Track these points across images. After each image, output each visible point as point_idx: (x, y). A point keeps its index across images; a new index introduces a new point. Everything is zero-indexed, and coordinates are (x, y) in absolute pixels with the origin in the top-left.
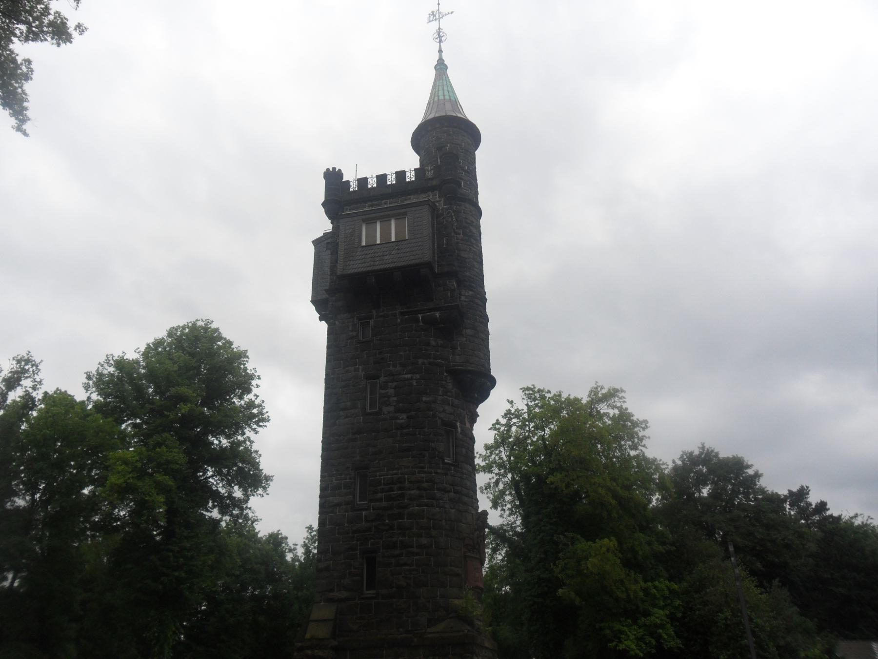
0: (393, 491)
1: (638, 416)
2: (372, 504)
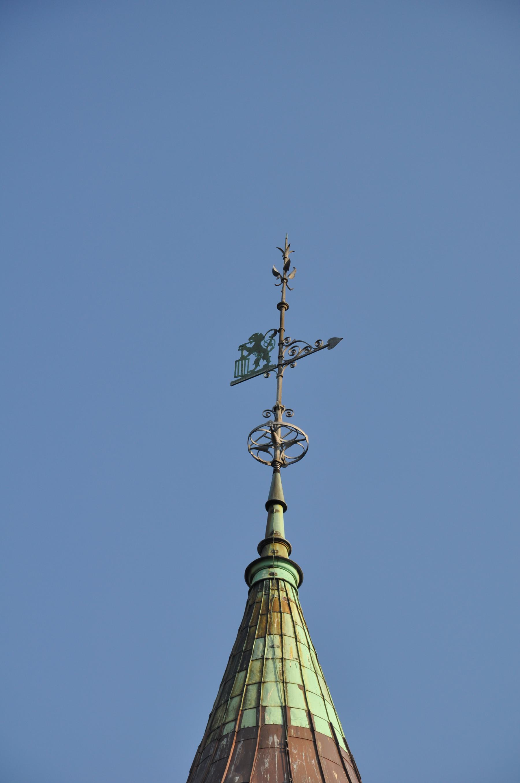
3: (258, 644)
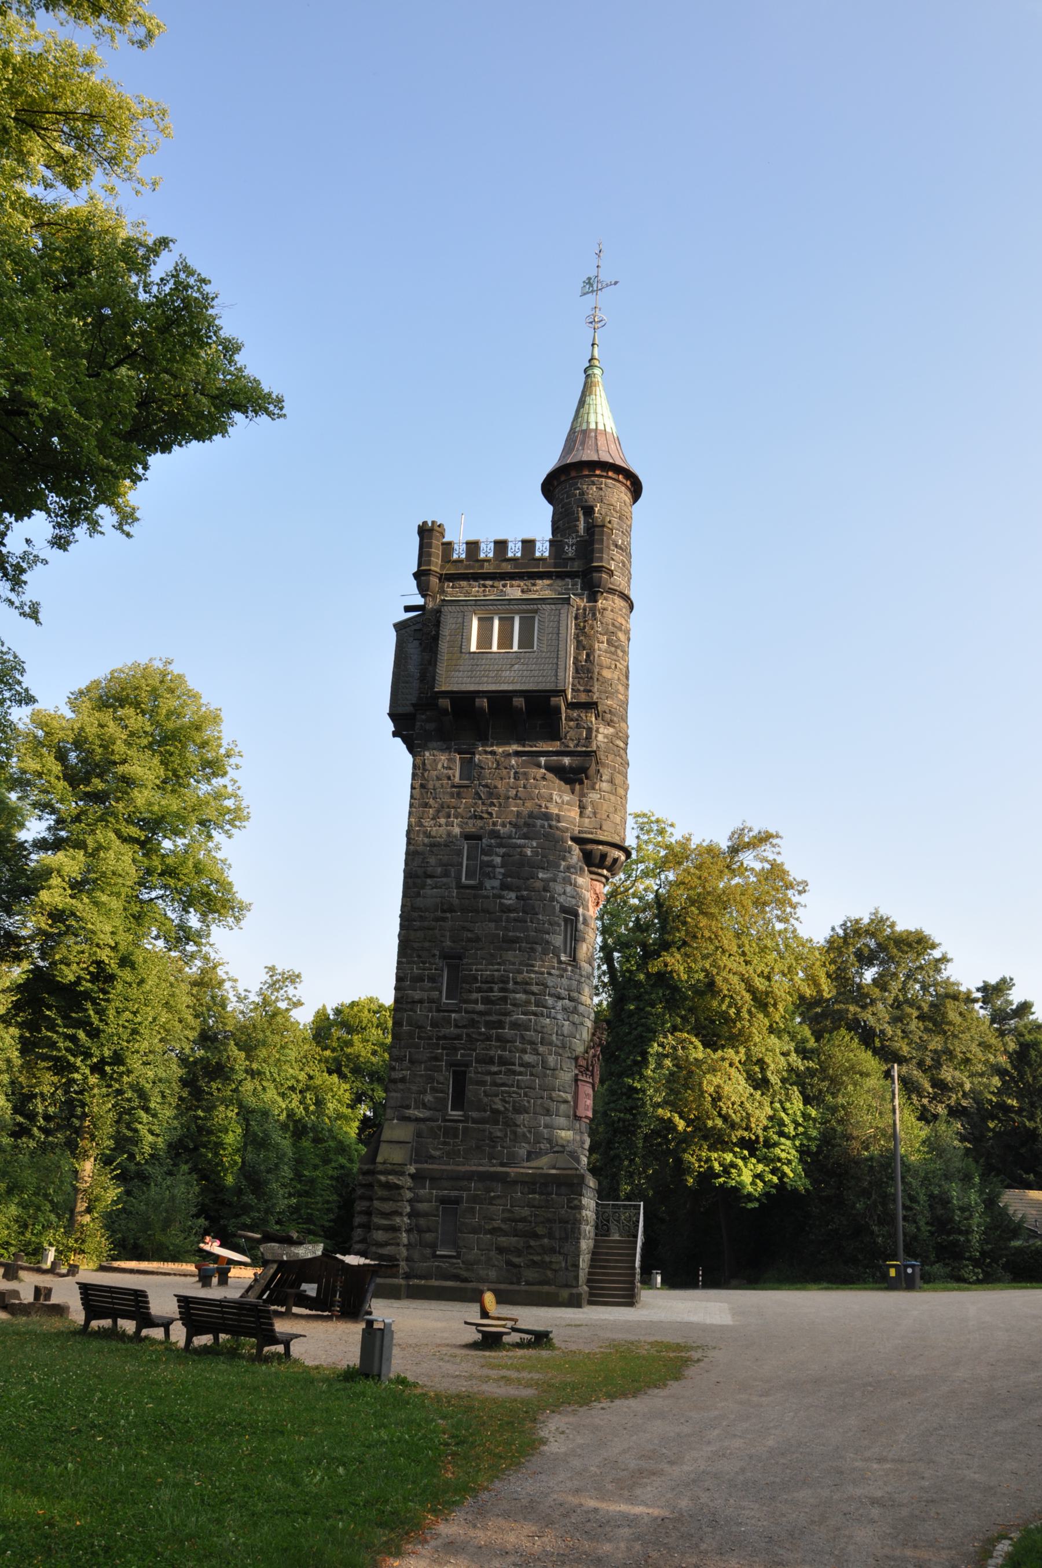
0: (492, 991)
1: (795, 872)
2: (464, 1006)
3: (587, 398)
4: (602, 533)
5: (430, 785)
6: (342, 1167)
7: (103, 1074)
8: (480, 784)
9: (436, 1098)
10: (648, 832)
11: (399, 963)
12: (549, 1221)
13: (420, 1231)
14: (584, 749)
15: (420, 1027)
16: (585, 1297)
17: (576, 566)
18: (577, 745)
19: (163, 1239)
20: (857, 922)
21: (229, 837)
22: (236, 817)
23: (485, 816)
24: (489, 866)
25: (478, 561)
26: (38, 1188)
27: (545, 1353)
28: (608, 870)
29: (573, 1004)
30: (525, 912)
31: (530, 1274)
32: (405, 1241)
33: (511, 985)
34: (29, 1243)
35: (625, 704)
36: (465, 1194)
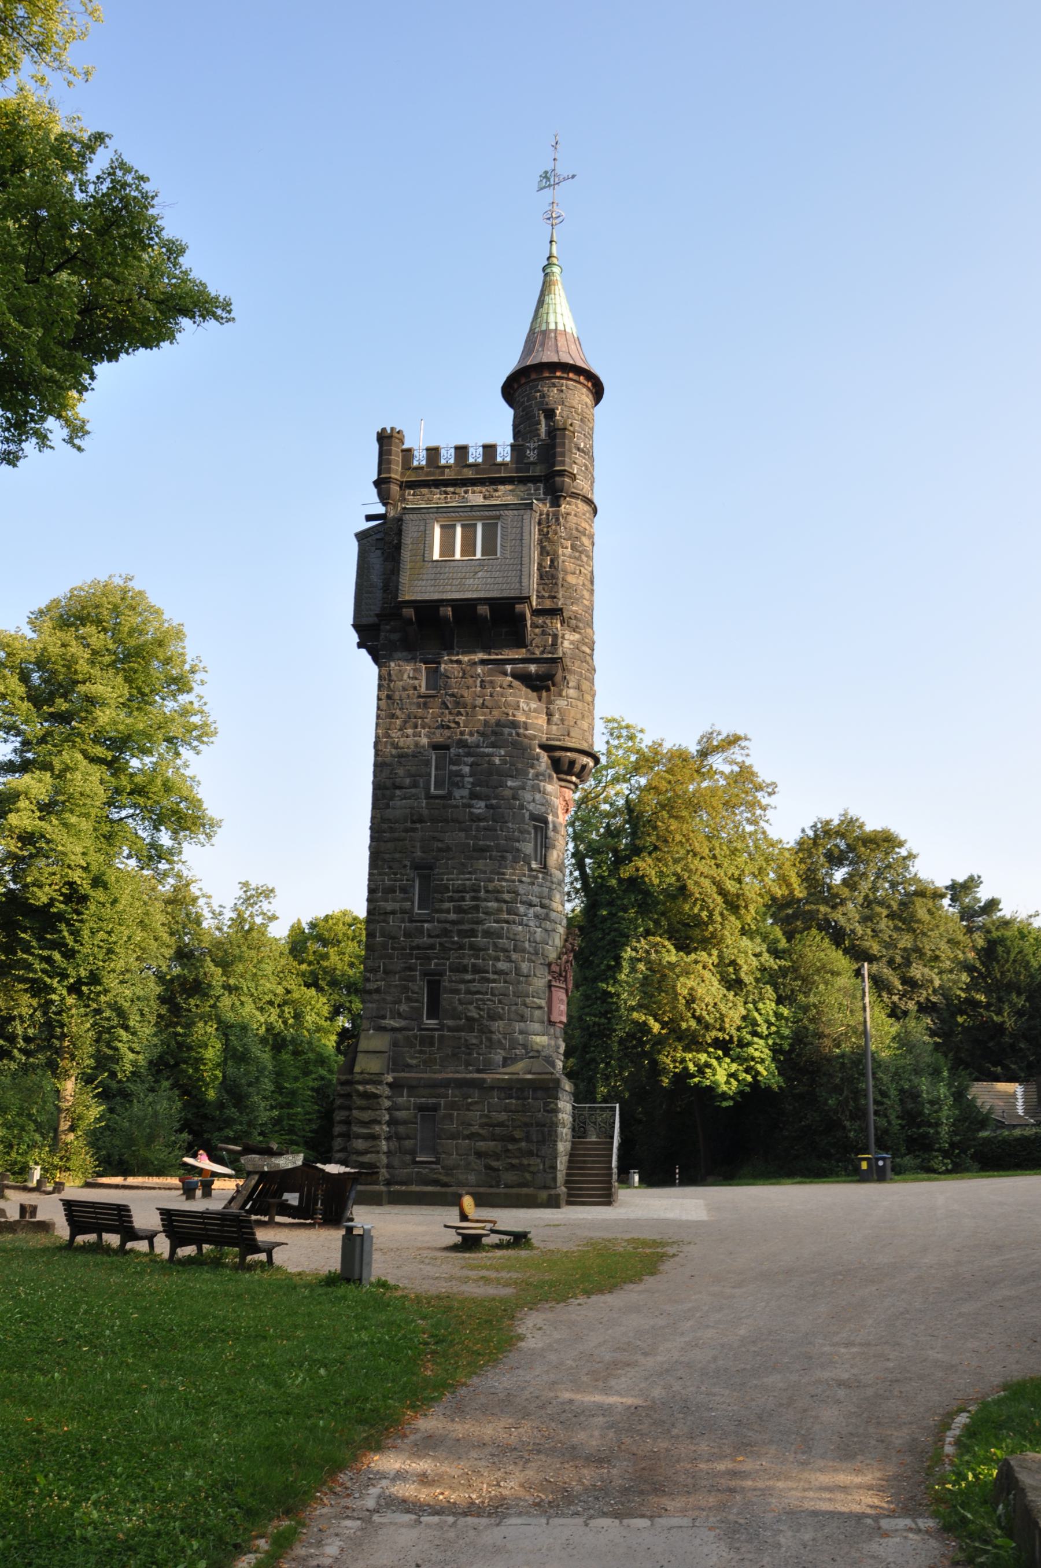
0: (464, 900)
1: (764, 775)
2: (436, 915)
3: (546, 298)
4: (564, 436)
5: (397, 696)
6: (322, 1078)
7: (80, 994)
8: (446, 694)
9: (412, 1007)
10: (618, 737)
11: (370, 874)
12: (526, 1125)
13: (399, 1138)
14: (550, 656)
15: (393, 938)
16: (563, 1198)
17: (538, 471)
18: (543, 652)
19: (148, 1155)
20: (828, 823)
21: (198, 753)
22: (203, 733)
23: (453, 725)
24: (457, 776)
25: (439, 467)
26: (21, 1108)
27: (523, 1253)
28: (578, 776)
29: (544, 911)
30: (494, 820)
31: (509, 1177)
32: (385, 1148)
33: (482, 894)
34: (15, 1163)
35: (590, 610)
36: (442, 1101)
